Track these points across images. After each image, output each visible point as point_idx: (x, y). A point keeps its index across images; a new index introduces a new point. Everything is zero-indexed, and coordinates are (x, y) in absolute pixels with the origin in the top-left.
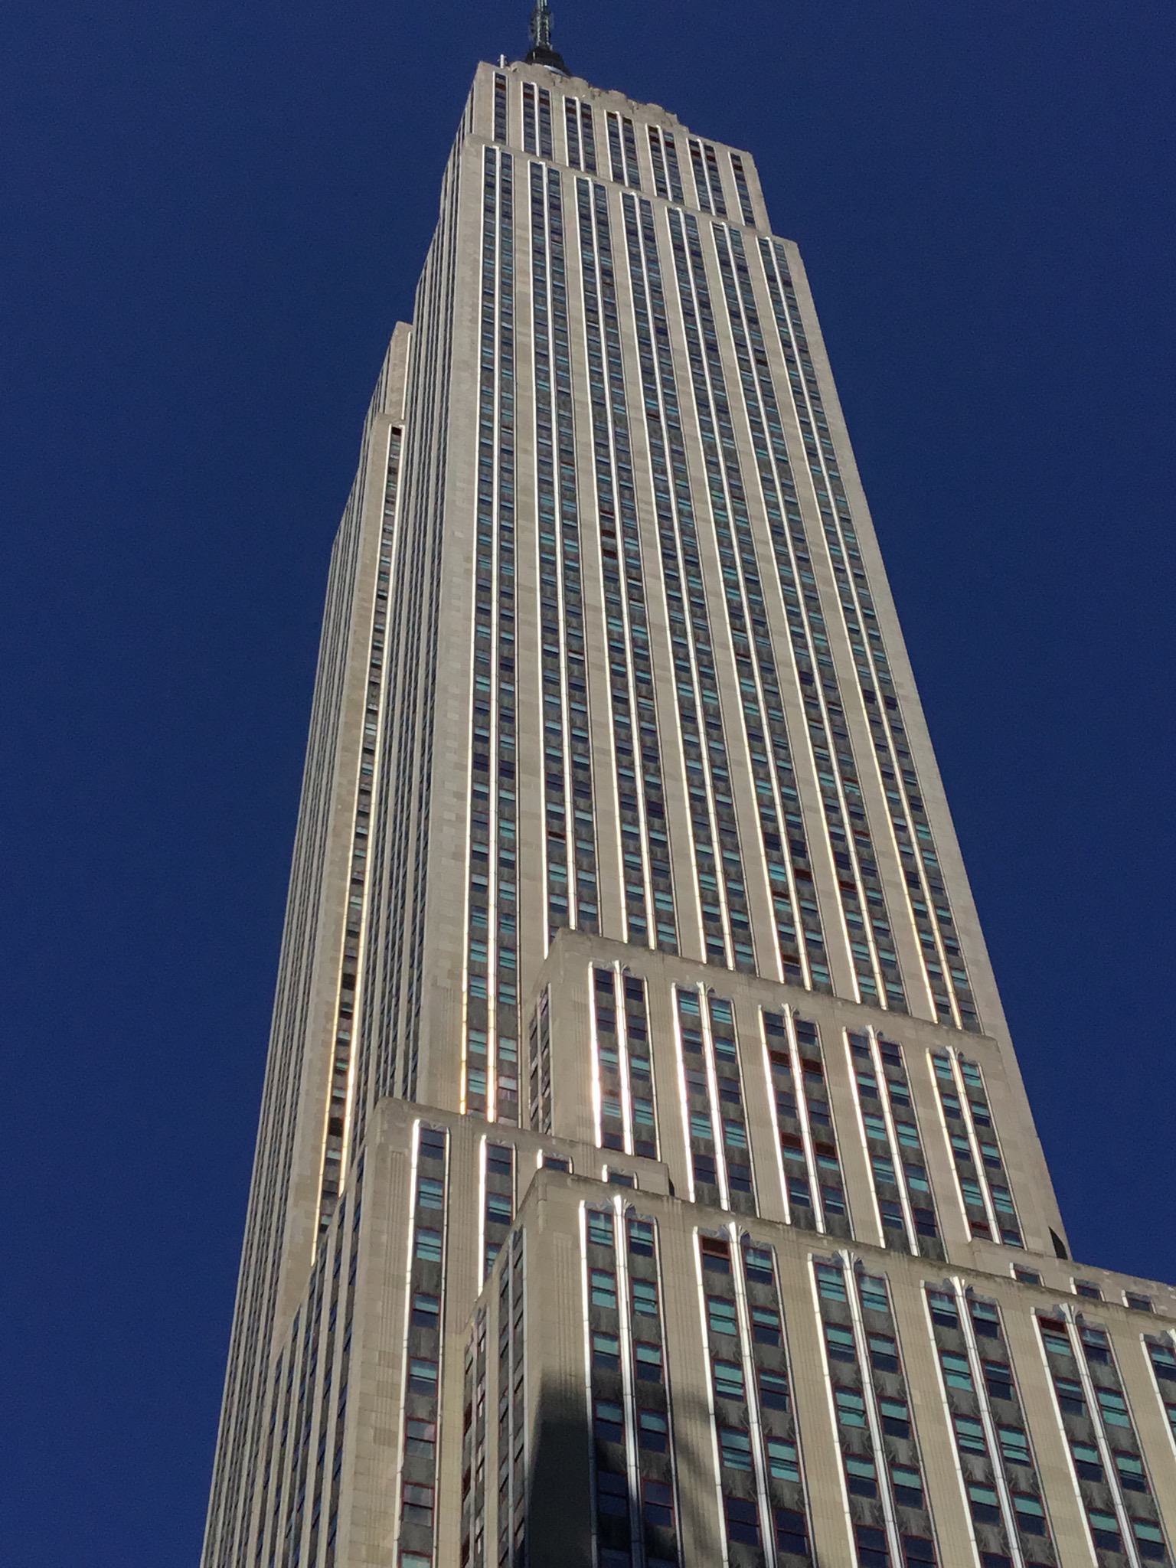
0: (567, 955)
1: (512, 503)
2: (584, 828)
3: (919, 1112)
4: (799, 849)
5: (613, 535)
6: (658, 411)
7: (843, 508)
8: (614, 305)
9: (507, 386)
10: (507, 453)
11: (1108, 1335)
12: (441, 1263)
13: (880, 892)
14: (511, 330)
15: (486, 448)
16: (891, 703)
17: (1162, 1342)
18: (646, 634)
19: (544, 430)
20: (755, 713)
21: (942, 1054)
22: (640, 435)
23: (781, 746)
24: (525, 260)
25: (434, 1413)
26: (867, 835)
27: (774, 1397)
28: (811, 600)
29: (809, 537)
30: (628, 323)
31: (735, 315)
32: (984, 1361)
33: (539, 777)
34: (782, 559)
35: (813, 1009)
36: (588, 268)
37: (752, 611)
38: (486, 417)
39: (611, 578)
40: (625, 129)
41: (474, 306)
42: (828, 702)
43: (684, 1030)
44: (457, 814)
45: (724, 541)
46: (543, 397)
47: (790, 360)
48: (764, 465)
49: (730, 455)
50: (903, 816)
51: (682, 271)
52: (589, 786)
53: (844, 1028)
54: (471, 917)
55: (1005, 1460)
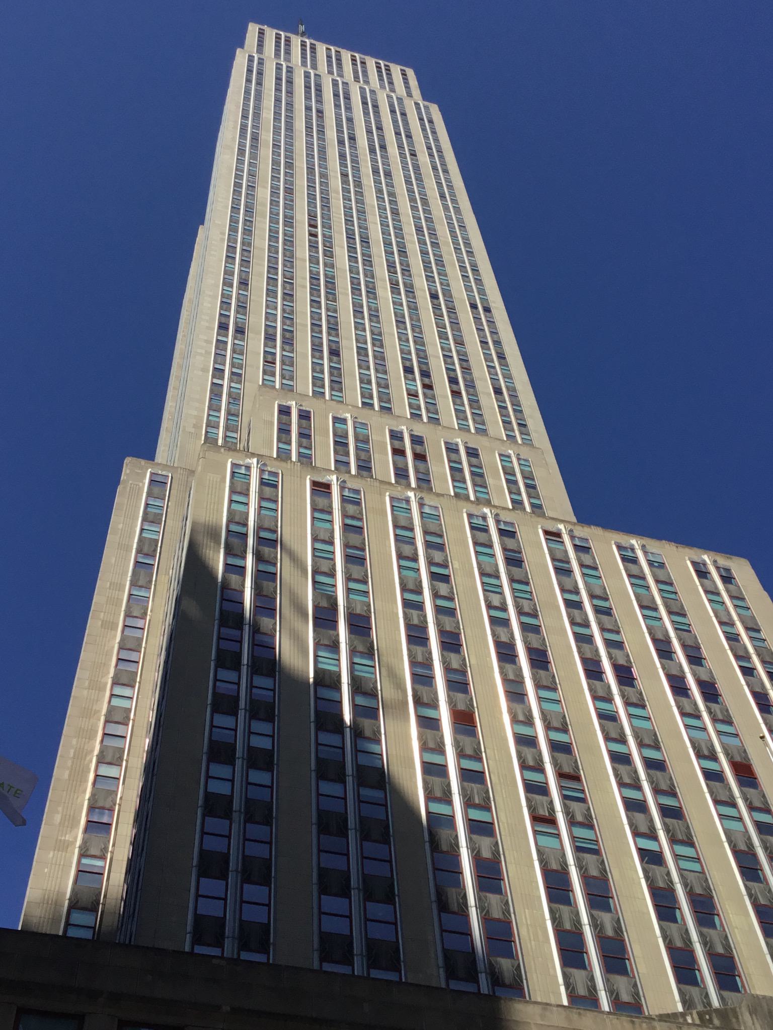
0: (261, 398)
1: (253, 209)
2: (288, 362)
3: (490, 481)
4: (425, 374)
5: (316, 227)
6: (348, 174)
7: (460, 221)
8: (324, 126)
9: (253, 156)
10: (251, 187)
11: (590, 541)
12: (158, 540)
13: (477, 396)
14: (258, 133)
15: (238, 185)
16: (487, 310)
17: (627, 545)
18: (334, 272)
19: (275, 178)
20: (401, 312)
21: (506, 454)
22: (336, 182)
23: (417, 328)
24: (269, 103)
25: (146, 614)
26: (470, 370)
27: (355, 559)
28: (440, 263)
29: (439, 233)
30: (331, 134)
31: (398, 134)
32: (505, 549)
33: (261, 335)
34: (422, 242)
35: (419, 430)
36: (308, 108)
37: (401, 264)
38: (239, 169)
39: (313, 246)
40: (336, 55)
41: (236, 122)
42: (447, 308)
43: (335, 435)
44: (206, 351)
45: (385, 233)
46: (276, 163)
47: (431, 155)
48: (412, 200)
49: (392, 194)
50: (492, 361)
51: (366, 113)
52: (293, 340)
53: (442, 439)
54: (211, 399)
55: (515, 598)
